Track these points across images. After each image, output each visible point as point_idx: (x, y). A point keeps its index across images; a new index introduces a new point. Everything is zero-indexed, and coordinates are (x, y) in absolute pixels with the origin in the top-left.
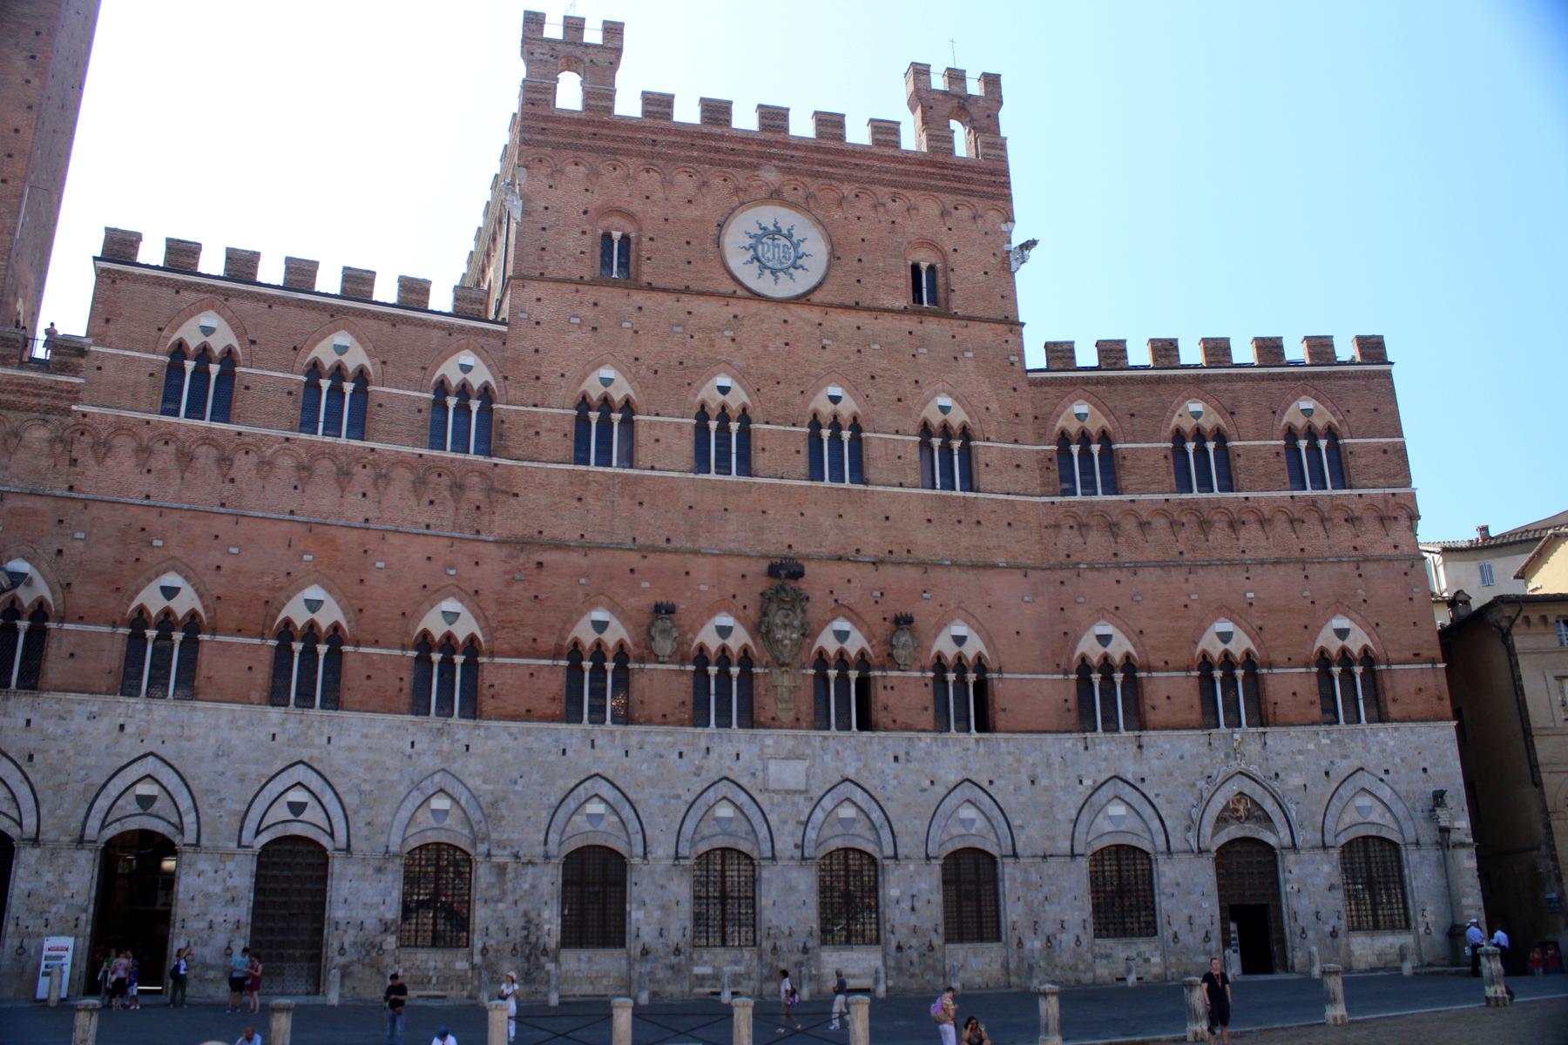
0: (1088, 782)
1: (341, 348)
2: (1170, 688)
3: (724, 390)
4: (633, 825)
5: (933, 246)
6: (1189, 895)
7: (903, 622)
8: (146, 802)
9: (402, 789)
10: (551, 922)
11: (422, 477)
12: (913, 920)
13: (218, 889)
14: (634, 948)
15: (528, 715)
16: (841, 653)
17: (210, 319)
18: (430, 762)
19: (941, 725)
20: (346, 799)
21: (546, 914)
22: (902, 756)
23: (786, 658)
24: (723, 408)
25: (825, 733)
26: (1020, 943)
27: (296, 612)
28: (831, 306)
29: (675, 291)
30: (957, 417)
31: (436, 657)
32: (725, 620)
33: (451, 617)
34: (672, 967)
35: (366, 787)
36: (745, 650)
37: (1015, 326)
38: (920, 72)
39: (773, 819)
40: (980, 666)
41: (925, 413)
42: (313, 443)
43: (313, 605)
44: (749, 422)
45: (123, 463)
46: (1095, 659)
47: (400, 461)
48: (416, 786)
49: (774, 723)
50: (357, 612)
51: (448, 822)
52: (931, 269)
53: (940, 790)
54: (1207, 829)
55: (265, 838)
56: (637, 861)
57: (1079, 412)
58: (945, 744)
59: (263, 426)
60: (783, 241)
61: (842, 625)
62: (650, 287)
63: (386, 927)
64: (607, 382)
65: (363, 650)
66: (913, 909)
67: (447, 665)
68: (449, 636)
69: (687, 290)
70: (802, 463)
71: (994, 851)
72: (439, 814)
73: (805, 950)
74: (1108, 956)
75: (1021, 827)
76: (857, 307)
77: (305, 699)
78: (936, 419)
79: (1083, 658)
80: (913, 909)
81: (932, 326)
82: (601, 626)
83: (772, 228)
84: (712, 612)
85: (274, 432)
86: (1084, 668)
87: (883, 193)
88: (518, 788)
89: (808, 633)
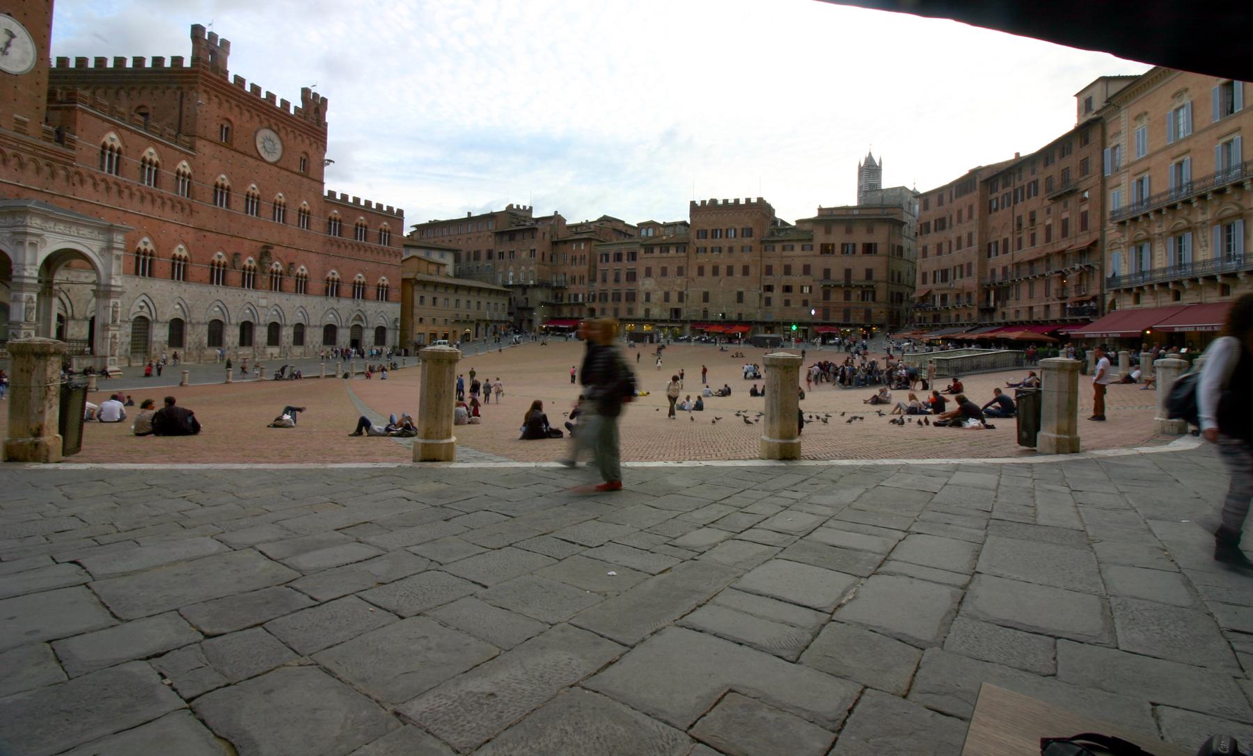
2: (346, 289)
5: (306, 153)
6: (344, 338)
7: (291, 264)
11: (175, 204)
17: (113, 135)
18: (176, 294)
30: (308, 208)
37: (323, 184)
43: (146, 243)
45: (89, 186)
50: (157, 246)
81: (305, 180)
86: (328, 280)
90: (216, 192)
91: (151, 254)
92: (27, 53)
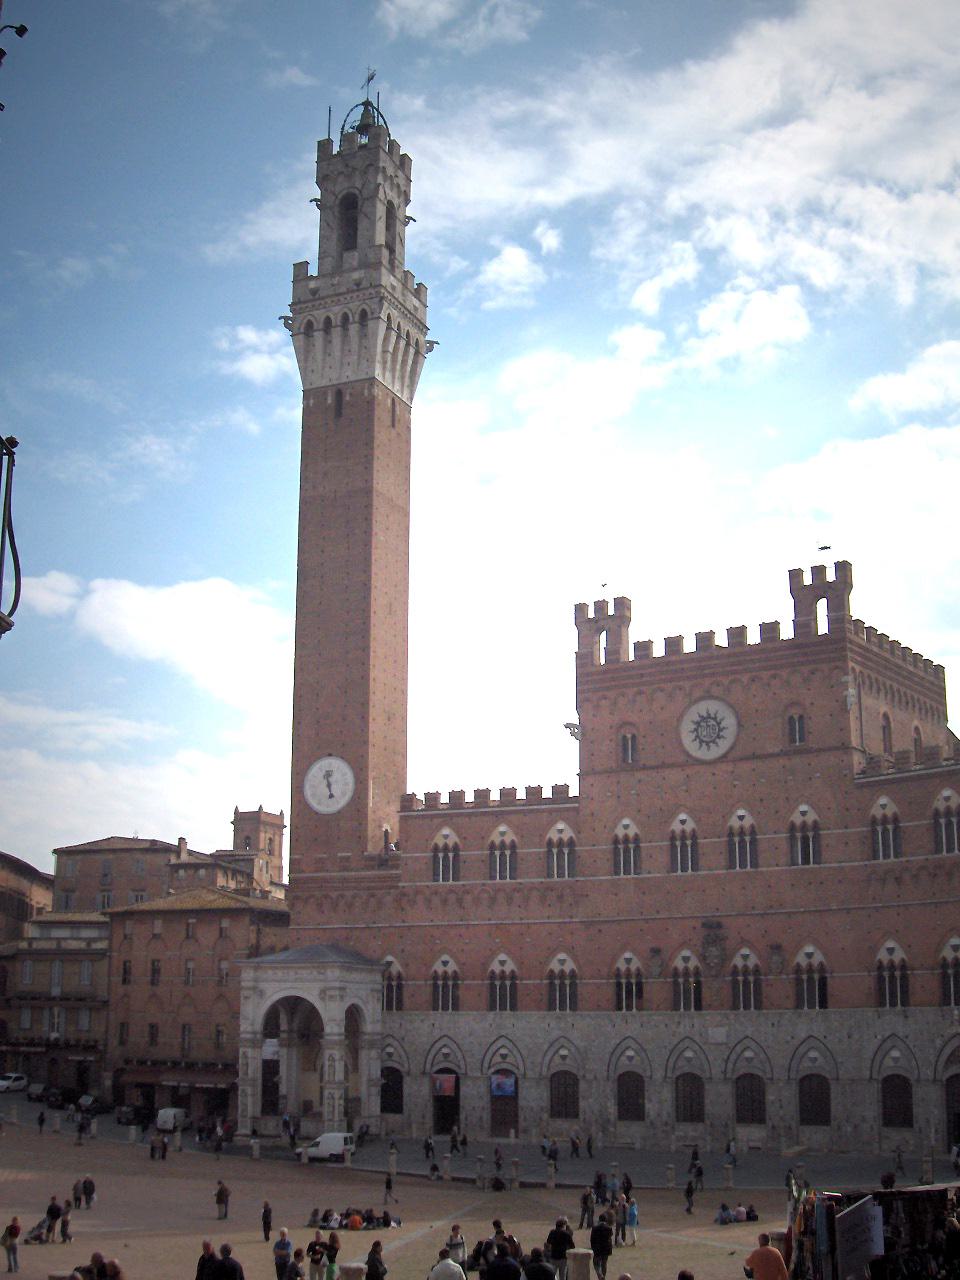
0: (879, 1037)
1: (503, 832)
3: (683, 822)
4: (646, 1061)
7: (777, 948)
8: (446, 1055)
9: (546, 1047)
10: (612, 1109)
12: (781, 1113)
13: (475, 1093)
14: (647, 1121)
15: (599, 1008)
16: (745, 966)
17: (446, 831)
18: (556, 1034)
19: (799, 1005)
20: (523, 1053)
21: (609, 1104)
22: (776, 1023)
23: (713, 973)
24: (683, 832)
25: (735, 1012)
26: (839, 1128)
27: (496, 967)
28: (741, 759)
29: (657, 767)
30: (811, 817)
31: (557, 982)
32: (686, 953)
33: (562, 962)
34: (663, 1131)
35: (531, 1046)
36: (697, 968)
38: (795, 575)
39: (711, 1058)
40: (822, 968)
41: (791, 819)
42: (494, 884)
43: (502, 963)
44: (697, 838)
46: (885, 962)
47: (532, 888)
48: (551, 1045)
49: (710, 1007)
50: (520, 963)
51: (568, 1061)
52: (801, 717)
53: (796, 1042)
54: (940, 1068)
55: (492, 1070)
56: (646, 1079)
57: (884, 805)
58: (800, 1016)
59: (472, 880)
60: (713, 722)
61: (745, 951)
62: (644, 768)
63: (542, 1109)
64: (626, 827)
65: (525, 982)
66: (781, 1107)
67: (562, 985)
68: (562, 971)
69: (663, 766)
70: (723, 860)
71: (828, 1076)
72: (564, 1057)
73: (726, 1125)
74: (887, 1138)
75: (842, 1063)
76: (754, 757)
77: (503, 1008)
78: (797, 819)
79: (880, 962)
80: (781, 1107)
81: (797, 760)
82: (628, 961)
83: (705, 715)
84: (682, 946)
85: (478, 882)
86: (880, 967)
87: (765, 674)
88: (595, 1044)
89: (726, 957)
90: (616, 851)
91: (513, 976)
92: (347, 784)
